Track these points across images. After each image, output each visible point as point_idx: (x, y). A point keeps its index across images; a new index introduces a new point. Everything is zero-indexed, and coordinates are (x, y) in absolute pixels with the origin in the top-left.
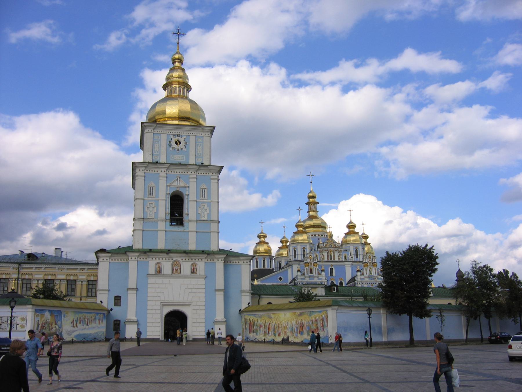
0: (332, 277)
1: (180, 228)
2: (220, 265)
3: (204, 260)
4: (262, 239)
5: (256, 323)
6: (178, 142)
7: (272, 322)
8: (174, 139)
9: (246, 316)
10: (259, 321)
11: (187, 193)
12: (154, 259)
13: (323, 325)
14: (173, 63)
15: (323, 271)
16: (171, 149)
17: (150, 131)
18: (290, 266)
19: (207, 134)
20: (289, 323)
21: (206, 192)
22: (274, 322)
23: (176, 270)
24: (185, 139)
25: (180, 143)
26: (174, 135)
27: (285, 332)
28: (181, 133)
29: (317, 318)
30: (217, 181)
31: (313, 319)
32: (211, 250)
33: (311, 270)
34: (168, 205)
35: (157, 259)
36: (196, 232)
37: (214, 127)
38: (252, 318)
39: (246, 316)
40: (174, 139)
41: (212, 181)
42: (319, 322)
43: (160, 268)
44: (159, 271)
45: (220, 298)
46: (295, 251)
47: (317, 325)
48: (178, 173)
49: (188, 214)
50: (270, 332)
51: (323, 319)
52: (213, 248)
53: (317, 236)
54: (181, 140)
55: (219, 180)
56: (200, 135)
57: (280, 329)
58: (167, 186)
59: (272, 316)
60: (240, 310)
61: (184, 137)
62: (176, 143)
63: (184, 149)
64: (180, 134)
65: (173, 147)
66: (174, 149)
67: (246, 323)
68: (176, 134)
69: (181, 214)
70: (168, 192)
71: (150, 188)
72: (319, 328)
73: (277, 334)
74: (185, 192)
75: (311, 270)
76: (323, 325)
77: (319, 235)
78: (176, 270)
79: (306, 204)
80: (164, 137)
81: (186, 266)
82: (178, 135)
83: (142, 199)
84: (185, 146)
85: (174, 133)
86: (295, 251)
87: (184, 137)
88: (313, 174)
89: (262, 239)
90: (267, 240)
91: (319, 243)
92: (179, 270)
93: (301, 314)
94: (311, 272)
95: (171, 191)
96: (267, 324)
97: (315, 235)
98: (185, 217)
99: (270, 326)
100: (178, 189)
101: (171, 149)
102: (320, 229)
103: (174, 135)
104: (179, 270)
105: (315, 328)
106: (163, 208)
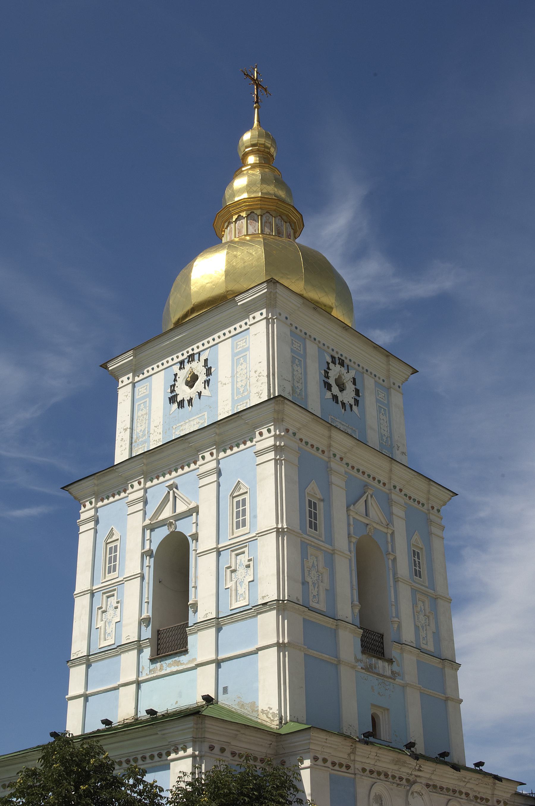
8: (332, 366)
16: (329, 395)
24: (354, 379)
54: (347, 378)
61: (352, 373)
80: (312, 349)
84: (357, 402)
87: (352, 373)
101: (329, 395)
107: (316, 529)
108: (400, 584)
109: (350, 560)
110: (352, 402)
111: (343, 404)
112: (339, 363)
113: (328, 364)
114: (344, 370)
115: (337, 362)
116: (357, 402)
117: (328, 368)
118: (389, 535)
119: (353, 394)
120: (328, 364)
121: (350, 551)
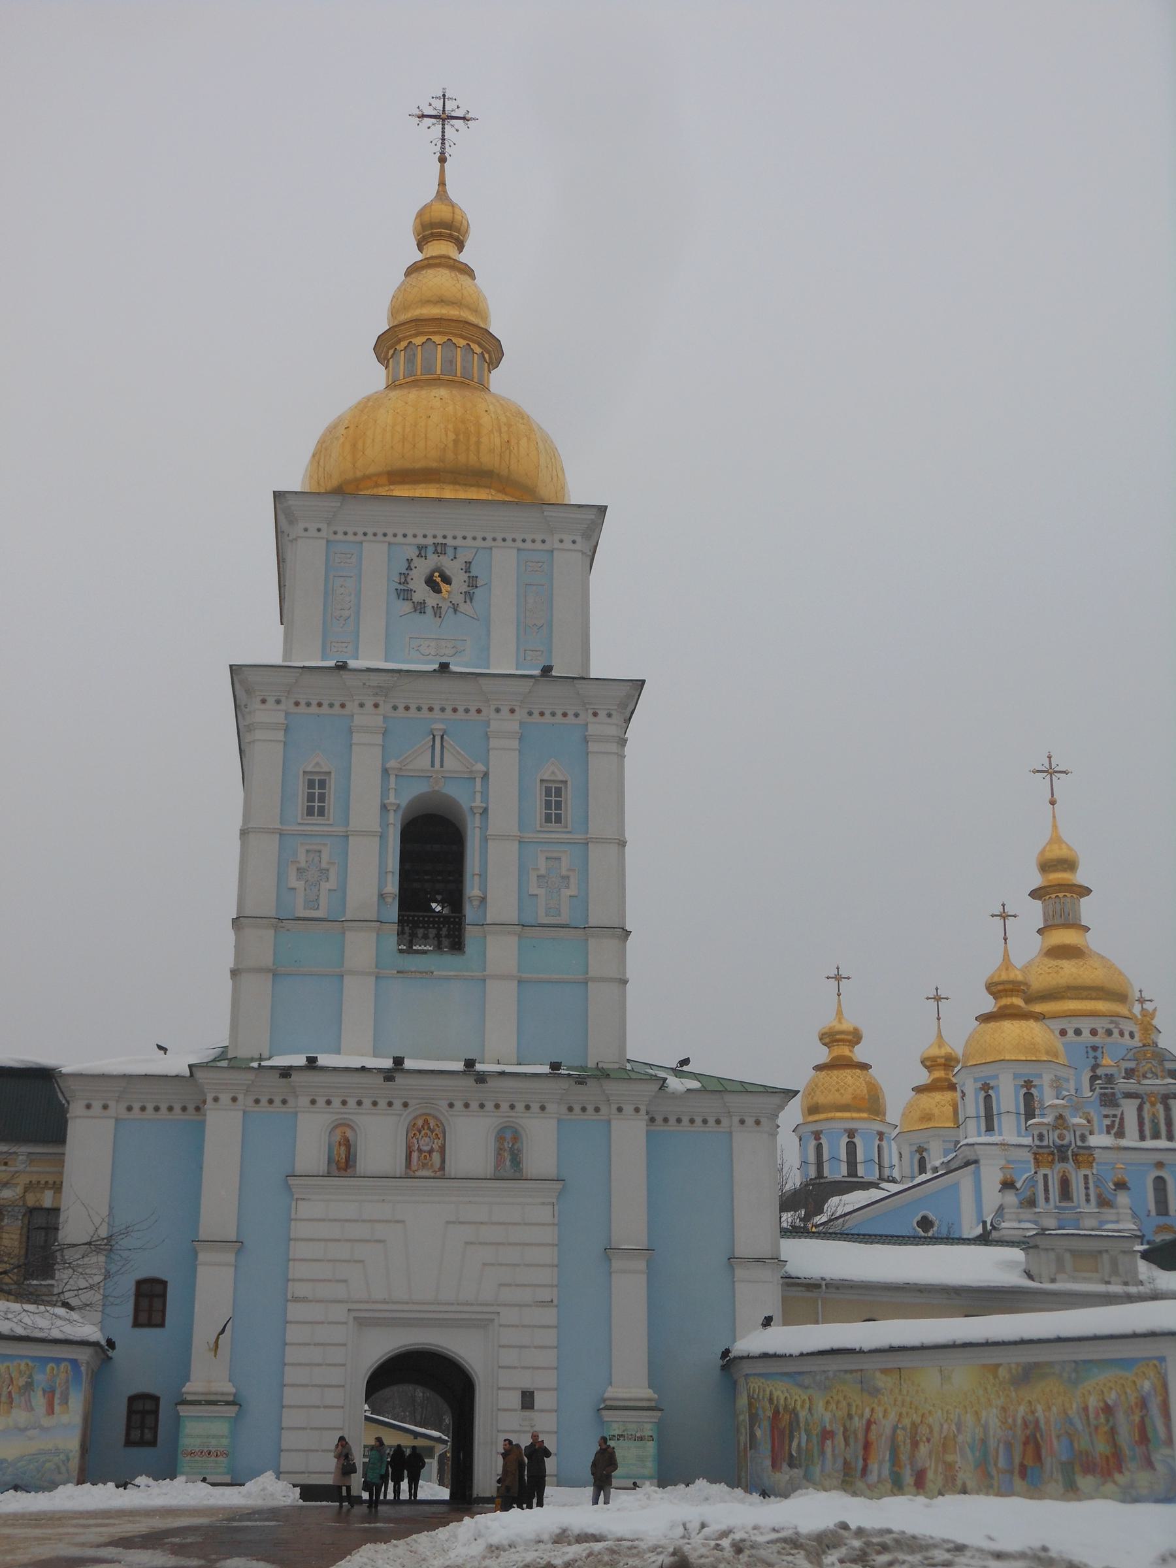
0: (1162, 1220)
1: (443, 963)
2: (629, 1136)
3: (551, 1107)
4: (845, 1051)
5: (803, 1414)
7: (879, 1414)
9: (755, 1384)
10: (820, 1405)
11: (478, 803)
12: (321, 1101)
13: (1143, 1437)
14: (420, 247)
15: (1121, 1185)
17: (312, 532)
18: (967, 1164)
19: (568, 538)
20: (969, 1419)
21: (570, 799)
22: (892, 1416)
23: (425, 1154)
25: (447, 580)
26: (422, 550)
27: (950, 1466)
29: (1111, 1397)
30: (613, 748)
31: (1093, 1402)
32: (591, 1064)
33: (1065, 1184)
34: (393, 862)
35: (336, 1102)
36: (520, 982)
37: (602, 510)
38: (781, 1391)
39: (755, 1384)
42: (1121, 1417)
43: (347, 1143)
44: (343, 1161)
45: (630, 1289)
46: (988, 1098)
47: (1113, 1432)
48: (437, 713)
49: (483, 900)
50: (874, 1467)
51: (1143, 1404)
52: (599, 1053)
53: (1086, 1033)
54: (453, 568)
55: (623, 742)
57: (923, 1449)
58: (385, 772)
59: (882, 1381)
60: (726, 1353)
62: (430, 582)
64: (450, 542)
65: (417, 597)
67: (753, 1419)
68: (430, 541)
69: (455, 900)
70: (392, 799)
71: (311, 784)
72: (1127, 1452)
73: (908, 1479)
74: (463, 797)
75: (1065, 1184)
76: (1143, 1437)
77: (1094, 1032)
78: (425, 1154)
79: (1035, 894)
81: (470, 1141)
82: (440, 549)
83: (272, 831)
85: (421, 541)
86: (988, 1098)
88: (1059, 763)
89: (845, 1051)
90: (860, 1053)
91: (1095, 1067)
92: (436, 1157)
93: (1027, 1375)
94: (1065, 1191)
95: (404, 796)
96: (858, 1424)
97: (1078, 1032)
98: (470, 913)
99: (873, 1436)
100: (436, 788)
101: (407, 607)
102: (1101, 1006)
103: (422, 550)
104: (436, 1157)
105: (1102, 1447)
106: (371, 872)
107: (321, 812)
108: (490, 843)
109: (382, 836)
110: (458, 599)
111: (437, 611)
112: (436, 552)
113: (409, 561)
115: (431, 549)
116: (469, 596)
117: (409, 568)
118: (478, 781)
119: (465, 588)
120: (409, 561)
121: (384, 824)
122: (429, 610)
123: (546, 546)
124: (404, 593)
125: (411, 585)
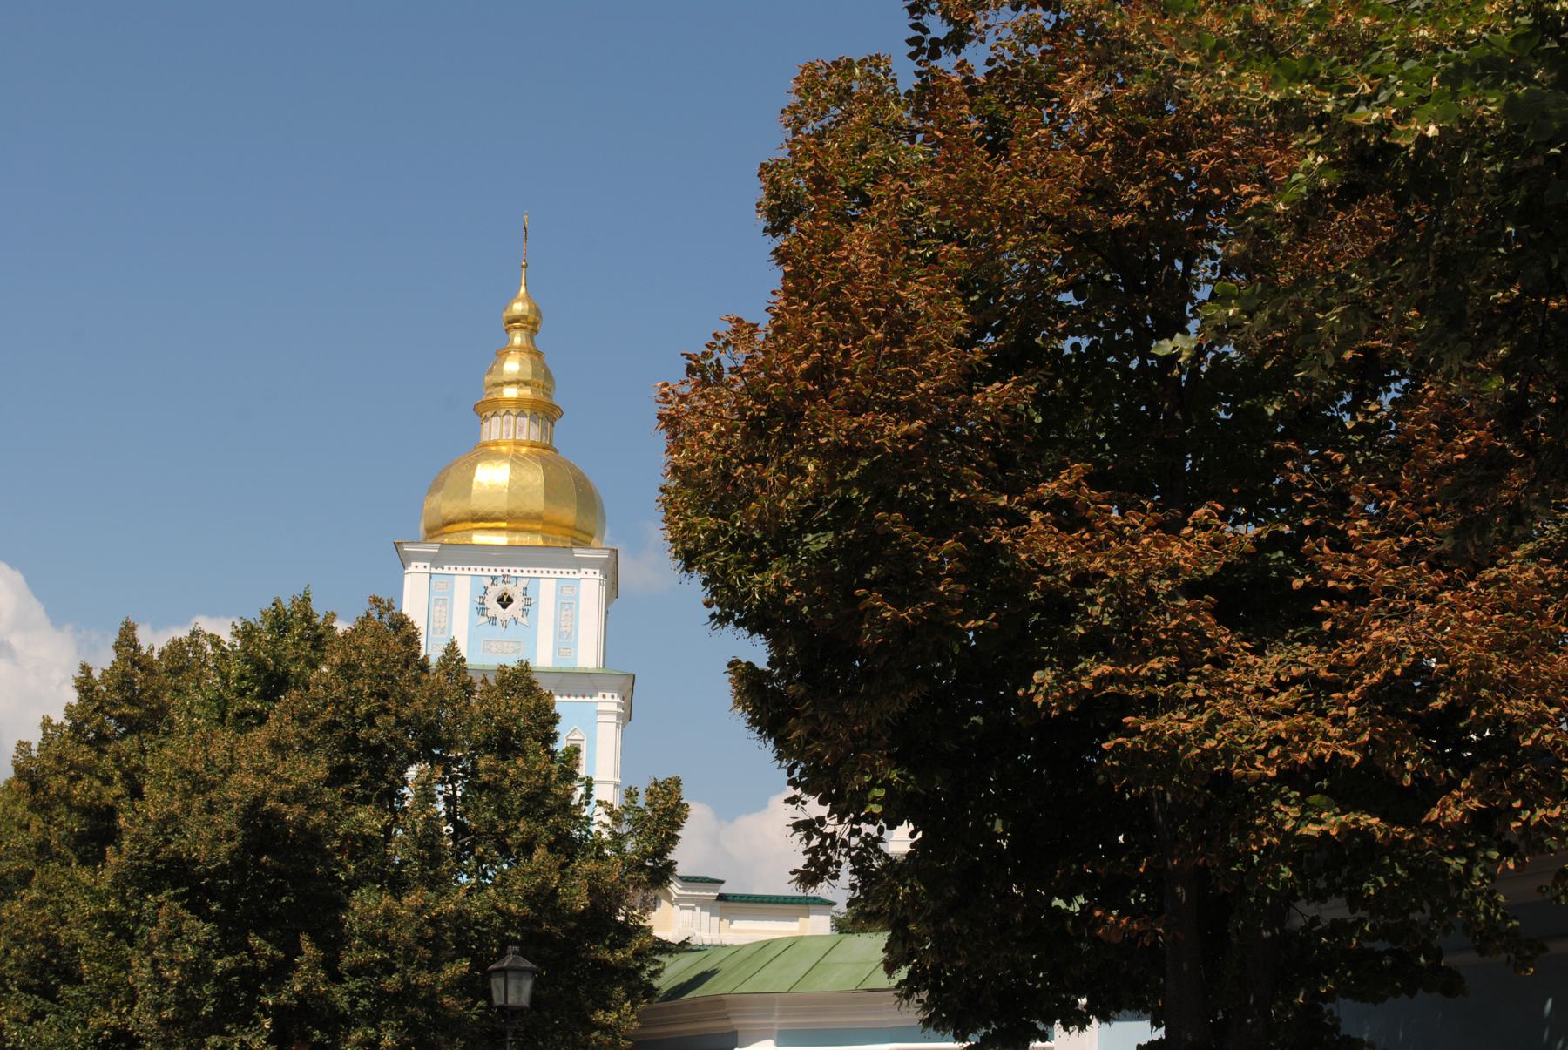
6: (505, 601)
19: (591, 571)
25: (510, 600)
26: (494, 578)
28: (515, 571)
40: (495, 592)
41: (600, 718)
54: (514, 591)
56: (571, 576)
62: (500, 600)
63: (524, 620)
65: (491, 613)
66: (493, 620)
68: (499, 573)
82: (506, 579)
84: (525, 611)
85: (493, 573)
101: (485, 619)
110: (518, 614)
114: (509, 586)
116: (525, 611)
122: (499, 622)
123: (578, 576)
124: (482, 610)
125: (487, 604)
